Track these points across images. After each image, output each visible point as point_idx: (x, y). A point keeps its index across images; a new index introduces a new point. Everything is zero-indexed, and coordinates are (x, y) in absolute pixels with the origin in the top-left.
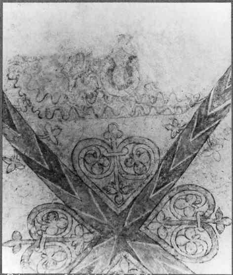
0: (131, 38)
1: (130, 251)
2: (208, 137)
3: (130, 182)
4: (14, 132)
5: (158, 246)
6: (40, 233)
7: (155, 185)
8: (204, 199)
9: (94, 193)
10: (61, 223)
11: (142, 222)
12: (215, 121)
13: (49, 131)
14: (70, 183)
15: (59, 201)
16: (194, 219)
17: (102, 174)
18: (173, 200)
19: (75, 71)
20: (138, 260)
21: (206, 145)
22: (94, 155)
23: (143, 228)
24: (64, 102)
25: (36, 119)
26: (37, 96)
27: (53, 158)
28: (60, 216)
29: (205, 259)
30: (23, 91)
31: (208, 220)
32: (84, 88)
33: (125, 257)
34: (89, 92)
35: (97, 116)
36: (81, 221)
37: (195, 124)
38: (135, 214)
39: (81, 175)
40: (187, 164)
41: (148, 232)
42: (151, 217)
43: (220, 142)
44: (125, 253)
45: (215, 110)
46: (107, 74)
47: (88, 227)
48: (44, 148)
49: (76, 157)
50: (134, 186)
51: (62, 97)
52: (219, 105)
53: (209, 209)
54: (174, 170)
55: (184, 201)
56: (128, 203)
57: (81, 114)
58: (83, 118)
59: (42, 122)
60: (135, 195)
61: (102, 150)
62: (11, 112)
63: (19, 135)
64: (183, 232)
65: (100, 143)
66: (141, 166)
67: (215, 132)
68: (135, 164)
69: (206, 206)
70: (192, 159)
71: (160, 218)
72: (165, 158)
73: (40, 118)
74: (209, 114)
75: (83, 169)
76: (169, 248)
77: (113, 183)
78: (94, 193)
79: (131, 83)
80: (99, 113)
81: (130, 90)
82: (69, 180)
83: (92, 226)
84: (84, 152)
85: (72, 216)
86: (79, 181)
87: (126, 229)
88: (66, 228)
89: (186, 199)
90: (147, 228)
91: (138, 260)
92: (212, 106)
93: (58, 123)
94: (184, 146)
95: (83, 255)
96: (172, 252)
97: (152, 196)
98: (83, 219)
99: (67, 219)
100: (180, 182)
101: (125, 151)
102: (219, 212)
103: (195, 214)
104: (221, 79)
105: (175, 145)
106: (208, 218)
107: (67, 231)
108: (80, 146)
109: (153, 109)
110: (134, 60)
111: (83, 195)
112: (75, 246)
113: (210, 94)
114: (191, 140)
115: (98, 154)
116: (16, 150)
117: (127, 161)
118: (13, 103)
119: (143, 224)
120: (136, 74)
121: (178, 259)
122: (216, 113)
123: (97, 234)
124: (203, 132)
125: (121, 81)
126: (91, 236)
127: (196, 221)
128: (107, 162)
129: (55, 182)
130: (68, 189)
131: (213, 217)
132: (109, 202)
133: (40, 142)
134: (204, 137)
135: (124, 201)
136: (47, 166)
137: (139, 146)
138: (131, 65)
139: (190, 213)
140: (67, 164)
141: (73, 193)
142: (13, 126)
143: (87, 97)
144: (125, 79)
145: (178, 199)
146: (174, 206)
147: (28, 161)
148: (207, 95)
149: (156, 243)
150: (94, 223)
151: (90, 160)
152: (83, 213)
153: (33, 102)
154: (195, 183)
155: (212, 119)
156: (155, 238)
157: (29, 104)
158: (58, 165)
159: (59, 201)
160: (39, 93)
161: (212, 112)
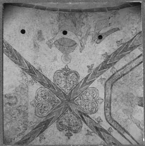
1: (74, 99)
2: (37, 70)
3: (52, 98)
4: (31, 138)
5: (73, 90)
6: (66, 127)
7: (53, 89)
8: (59, 74)
9: (54, 110)
10: (64, 121)
11: (65, 95)
12: (31, 67)
13: (31, 126)
14: (50, 117)
15: (56, 121)
16: (65, 78)
17: (47, 107)
18: (58, 84)
19: (10, 118)
20: (77, 96)
21: (40, 71)
23: (67, 94)
24: (21, 121)
25: (27, 130)
26: (18, 131)
27: (41, 124)
28: (61, 121)
29: (78, 76)
30: (16, 136)
31: (66, 73)
32: (16, 114)
33: (76, 100)
34: (18, 112)
35: (27, 109)
36: (63, 114)
37: (32, 74)
38: (62, 97)
39: (47, 114)
40: (46, 78)
41: (68, 93)
42: (64, 92)
43: (39, 66)
44: (75, 101)
45: (27, 66)
46: (11, 106)
47: (65, 112)
49: (41, 116)
50: (53, 96)
51: (19, 122)
52: (25, 65)
53: (62, 72)
54: (48, 83)
55: (59, 80)
56: (58, 99)
57: (26, 114)
58: (28, 114)
59: (28, 128)
60: (56, 96)
61: (39, 107)
62: (24, 139)
63: (32, 136)
64: (69, 82)
65: (37, 107)
66: (46, 94)
67: (35, 67)
69: (61, 73)
70: (44, 76)
71: (64, 89)
72: (44, 85)
73: (26, 129)
74: (28, 69)
75: (45, 113)
76: (74, 87)
77: (51, 103)
78: (54, 110)
79: (15, 97)
80: (26, 108)
81: (18, 97)
82: (49, 118)
83: (65, 111)
84: (39, 113)
85: (61, 117)
86: (49, 115)
87: (67, 100)
88: (65, 119)
89: (58, 80)
90: (67, 93)
91: (77, 96)
92: (25, 67)
93: (29, 123)
94: (40, 79)
95: (74, 114)
96: (75, 86)
97: (57, 91)
98: (62, 114)
99: (62, 119)
100: (52, 81)
101: (40, 99)
102: (63, 69)
103: (64, 77)
104: (16, 63)
105: (39, 82)
106: (65, 73)
107: (66, 118)
108: (38, 115)
109: (26, 89)
110: (6, 96)
111: (55, 113)
112: (71, 116)
113: (21, 68)
114: (38, 76)
115: (41, 108)
116: (37, 137)
117: (44, 99)
119: (65, 94)
120: (12, 95)
121: (78, 84)
122: (28, 66)
123: (68, 109)
124: (35, 71)
125: (14, 100)
126: (68, 111)
127: (66, 77)
128: (44, 105)
129: (49, 123)
130: (52, 118)
131: (65, 71)
132: (58, 105)
133: (35, 129)
134: (37, 71)
135: (58, 100)
136: (44, 126)
137: (39, 94)
138: (8, 97)
139: (63, 79)
140: (43, 119)
141: (54, 117)
142: (29, 138)
143: (20, 113)
144: (13, 99)
145: (58, 82)
146: (60, 84)
147: (42, 132)
148: (21, 69)
149: (72, 91)
151: (42, 111)
152: (61, 113)
153: (21, 132)
154: (53, 76)
155: (31, 68)
156: (70, 91)
157: (21, 134)
158: (43, 122)
159: (56, 121)
160: (17, 130)
161: (28, 67)
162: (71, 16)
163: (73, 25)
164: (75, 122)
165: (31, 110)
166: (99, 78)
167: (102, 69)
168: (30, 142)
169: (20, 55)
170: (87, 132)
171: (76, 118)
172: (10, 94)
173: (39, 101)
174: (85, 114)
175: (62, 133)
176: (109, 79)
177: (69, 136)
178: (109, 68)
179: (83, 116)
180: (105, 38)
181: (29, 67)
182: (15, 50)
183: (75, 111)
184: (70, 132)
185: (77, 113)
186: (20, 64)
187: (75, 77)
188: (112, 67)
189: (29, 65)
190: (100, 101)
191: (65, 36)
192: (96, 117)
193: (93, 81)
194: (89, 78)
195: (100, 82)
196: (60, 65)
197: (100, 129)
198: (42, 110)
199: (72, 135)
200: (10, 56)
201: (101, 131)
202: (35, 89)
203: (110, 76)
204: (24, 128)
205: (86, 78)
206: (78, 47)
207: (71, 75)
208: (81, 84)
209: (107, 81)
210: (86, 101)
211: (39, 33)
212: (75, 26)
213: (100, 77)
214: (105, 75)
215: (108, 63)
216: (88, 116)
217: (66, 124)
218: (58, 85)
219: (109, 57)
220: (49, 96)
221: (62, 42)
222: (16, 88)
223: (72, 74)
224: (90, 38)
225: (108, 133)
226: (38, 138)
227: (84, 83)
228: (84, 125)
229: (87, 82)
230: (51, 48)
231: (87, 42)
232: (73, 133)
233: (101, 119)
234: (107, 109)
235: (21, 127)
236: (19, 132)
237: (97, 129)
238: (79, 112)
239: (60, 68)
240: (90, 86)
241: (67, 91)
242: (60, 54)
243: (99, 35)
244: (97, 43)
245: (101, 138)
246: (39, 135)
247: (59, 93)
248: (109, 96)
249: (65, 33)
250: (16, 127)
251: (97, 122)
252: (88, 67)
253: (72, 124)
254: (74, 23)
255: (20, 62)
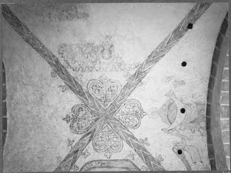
0: (111, 37)
1: (109, 124)
2: (141, 80)
7: (119, 99)
10: (84, 112)
14: (87, 97)
19: (87, 51)
22: (96, 86)
25: (72, 71)
32: (91, 58)
34: (93, 60)
35: (97, 70)
38: (111, 110)
39: (91, 93)
46: (101, 53)
48: (76, 83)
50: (112, 99)
54: (126, 93)
58: (91, 71)
59: (75, 72)
62: (62, 67)
68: (112, 90)
71: (120, 111)
72: (124, 88)
74: (142, 71)
77: (103, 98)
80: (98, 69)
84: (92, 85)
86: (90, 96)
87: (107, 116)
92: (144, 68)
93: (81, 73)
96: (124, 124)
100: (129, 98)
101: (108, 85)
102: (142, 110)
108: (90, 83)
110: (112, 47)
111: (92, 101)
114: (134, 81)
116: (65, 83)
118: (62, 64)
120: (113, 54)
128: (101, 89)
129: (81, 96)
130: (86, 99)
132: (102, 105)
133: (74, 80)
138: (111, 49)
140: (85, 88)
142: (63, 74)
144: (108, 55)
147: (70, 88)
149: (118, 121)
150: (96, 112)
151: (95, 88)
152: (92, 109)
155: (143, 74)
156: (118, 119)
157: (69, 65)
161: (144, 70)
162: (201, 118)
163: (192, 120)
164: (83, 126)
165: (96, 75)
166: (134, 152)
167: (144, 155)
168: (59, 74)
169: (158, 61)
170: (71, 140)
171: (87, 126)
172: (114, 51)
173: (106, 83)
174: (92, 137)
175: (70, 111)
176: (134, 164)
177: (67, 119)
178: (147, 164)
179: (90, 135)
180: (179, 157)
181: (144, 72)
182: (163, 56)
183: (95, 125)
184: (71, 121)
185: (93, 127)
186: (148, 62)
187: (134, 124)
188: (147, 167)
189: (146, 72)
190: (108, 154)
191: (179, 112)
192: (89, 151)
193: (131, 146)
194: (133, 140)
195: (129, 154)
196: (146, 107)
197: (75, 155)
198: (95, 87)
199: (67, 123)
200: (158, 50)
201: (74, 158)
202: (120, 79)
203: (137, 165)
204: (75, 67)
205: (133, 138)
206: (167, 126)
207: (136, 119)
208: (127, 132)
209: (131, 162)
210: (107, 138)
211: (183, 81)
212: (191, 122)
213: (136, 153)
214: (138, 159)
215: (152, 162)
216: (90, 141)
217: (80, 115)
218: (125, 104)
219: (159, 164)
220: (112, 95)
221: (173, 108)
222: (121, 58)
223: (137, 121)
224: (179, 140)
225: (72, 165)
226: (63, 84)
227: (127, 134)
228: (80, 136)
229: (129, 138)
230: (166, 95)
231: (174, 137)
232: (70, 123)
233: (87, 156)
234: (100, 164)
235: (77, 64)
236: (70, 61)
237: (77, 151)
238: (95, 130)
239: (143, 107)
240: (125, 143)
241: (118, 115)
242: (159, 105)
243: (183, 151)
244: (173, 149)
245: (66, 157)
246: (67, 84)
247: (115, 107)
248: (115, 166)
249: (183, 111)
250: (76, 59)
251: (84, 151)
252: (146, 139)
253: (80, 123)
254: (194, 121)
255: (151, 61)
